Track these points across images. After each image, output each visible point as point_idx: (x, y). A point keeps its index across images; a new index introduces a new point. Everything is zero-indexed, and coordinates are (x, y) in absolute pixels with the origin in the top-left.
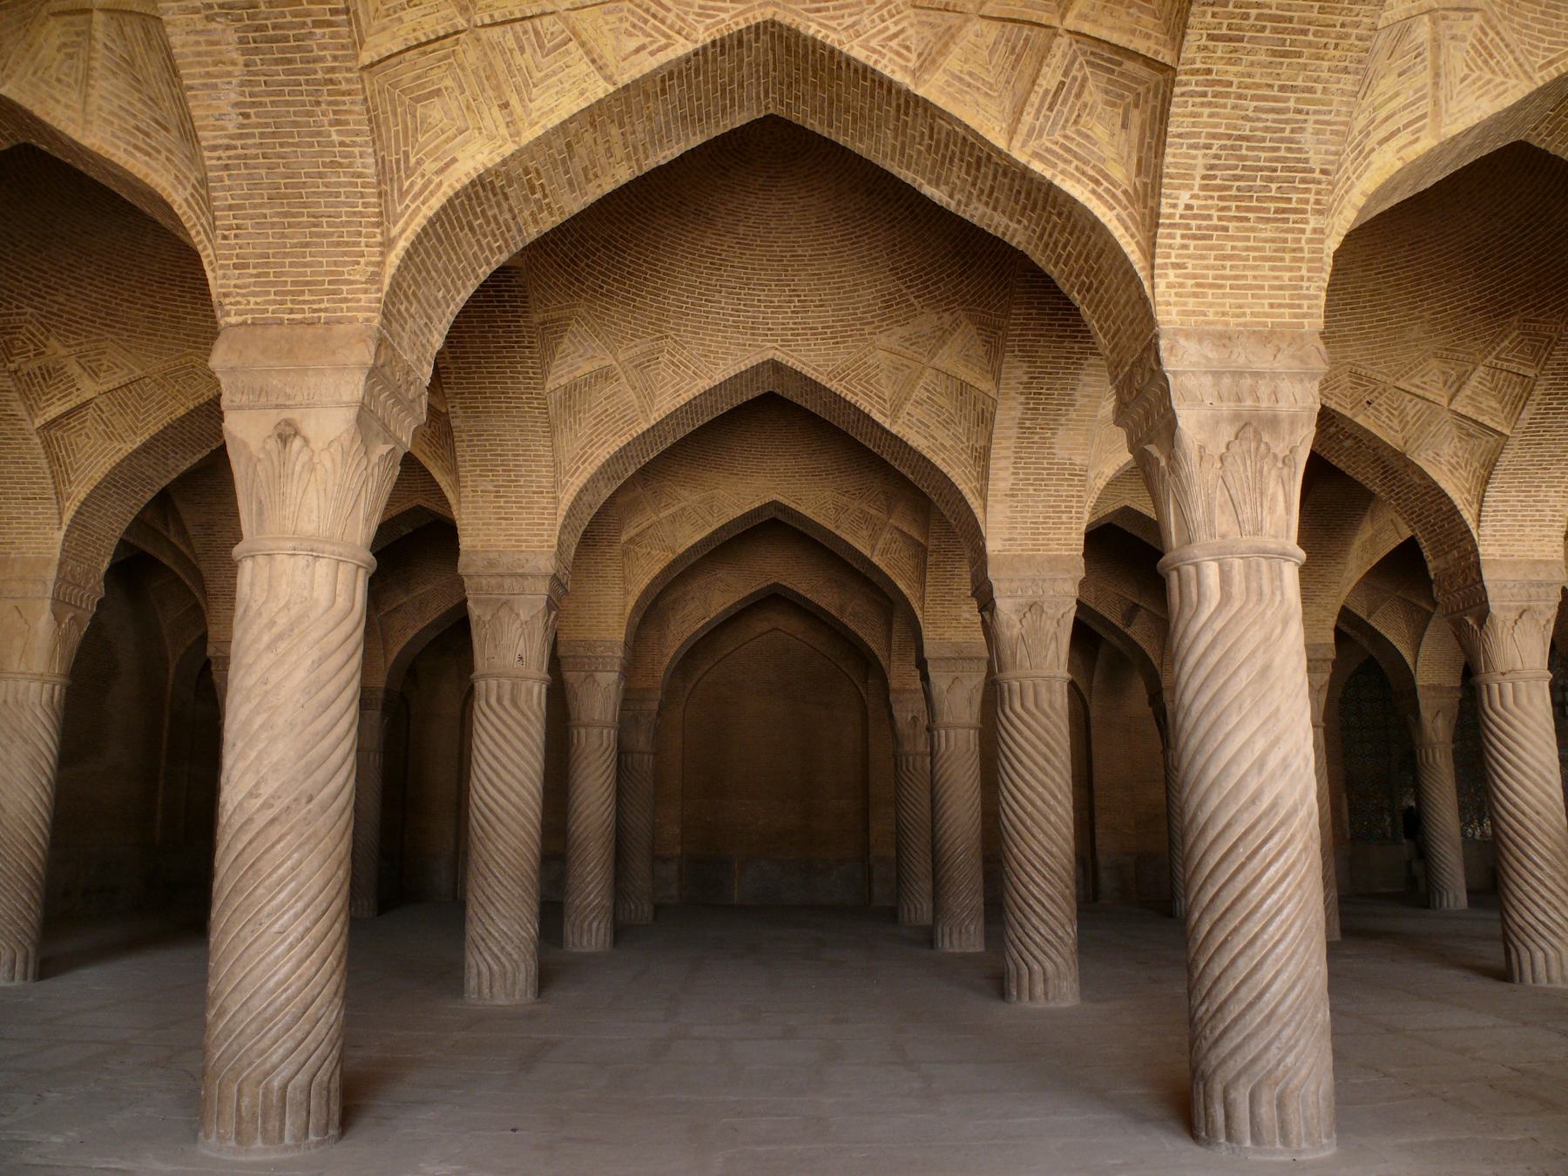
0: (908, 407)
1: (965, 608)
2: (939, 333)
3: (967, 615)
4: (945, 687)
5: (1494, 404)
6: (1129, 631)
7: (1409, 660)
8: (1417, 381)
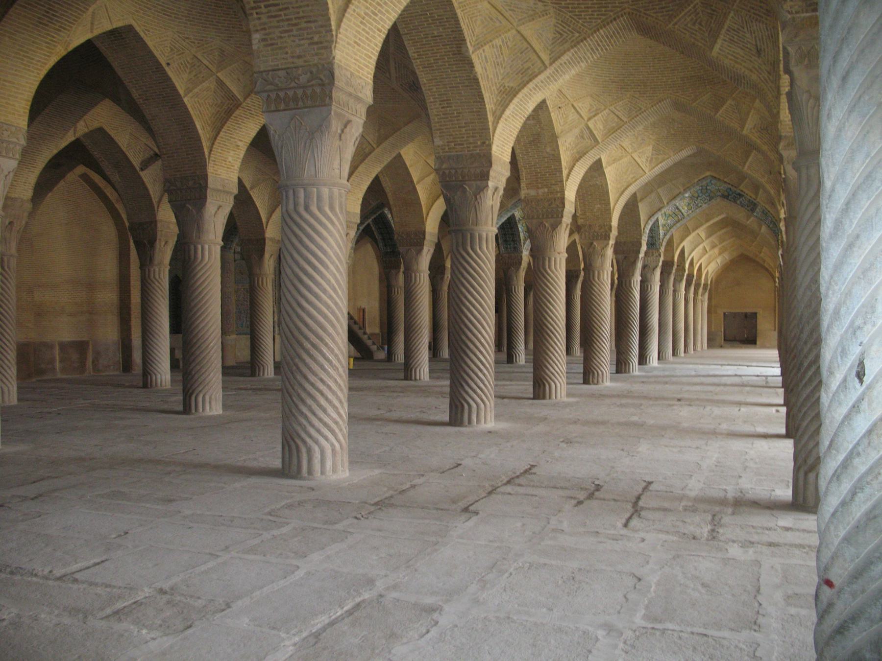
0: (486, 48)
1: (232, 153)
2: (532, 13)
3: (230, 159)
4: (213, 212)
5: (601, 127)
6: (142, 174)
7: (264, 220)
8: (580, 105)
